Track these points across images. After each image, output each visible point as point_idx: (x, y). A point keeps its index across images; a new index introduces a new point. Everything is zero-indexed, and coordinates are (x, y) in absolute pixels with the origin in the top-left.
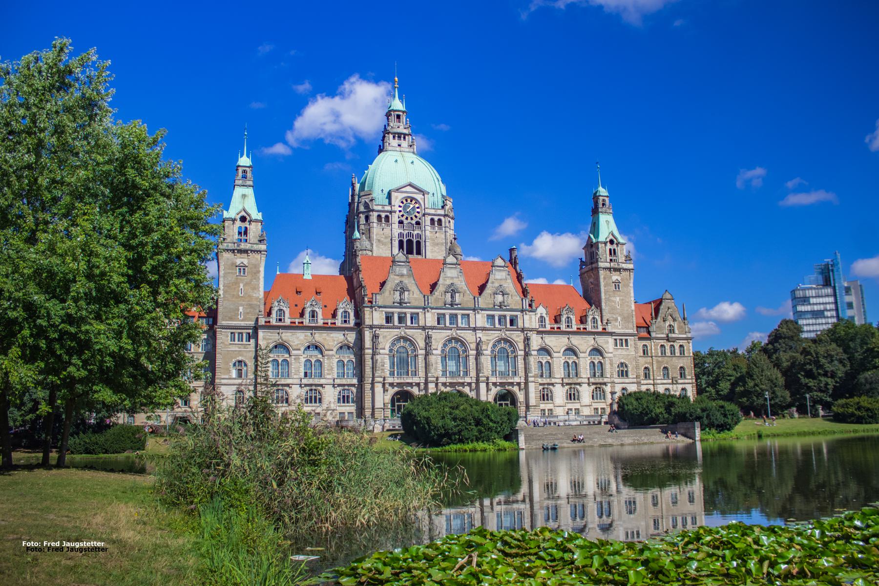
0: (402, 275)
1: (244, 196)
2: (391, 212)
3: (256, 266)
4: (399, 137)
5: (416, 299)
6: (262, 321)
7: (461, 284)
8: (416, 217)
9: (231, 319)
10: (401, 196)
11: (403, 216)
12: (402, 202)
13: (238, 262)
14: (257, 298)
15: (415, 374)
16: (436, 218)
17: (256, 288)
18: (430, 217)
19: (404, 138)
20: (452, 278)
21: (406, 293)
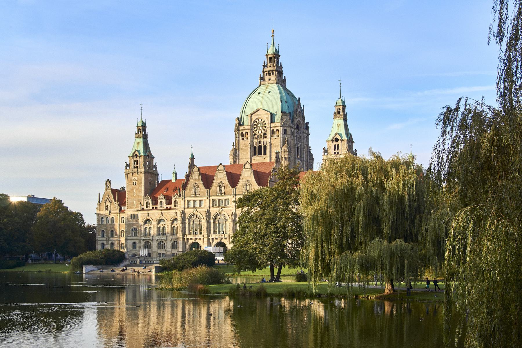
0: (195, 180)
1: (138, 143)
2: (248, 129)
3: (141, 180)
4: (269, 74)
5: (202, 192)
6: (140, 208)
7: (226, 181)
8: (264, 130)
9: (131, 207)
10: (254, 118)
11: (256, 131)
12: (256, 122)
13: (133, 178)
14: (141, 196)
15: (201, 233)
16: (275, 130)
17: (140, 191)
18: (272, 129)
19: (273, 75)
20: (221, 179)
21: (197, 189)
